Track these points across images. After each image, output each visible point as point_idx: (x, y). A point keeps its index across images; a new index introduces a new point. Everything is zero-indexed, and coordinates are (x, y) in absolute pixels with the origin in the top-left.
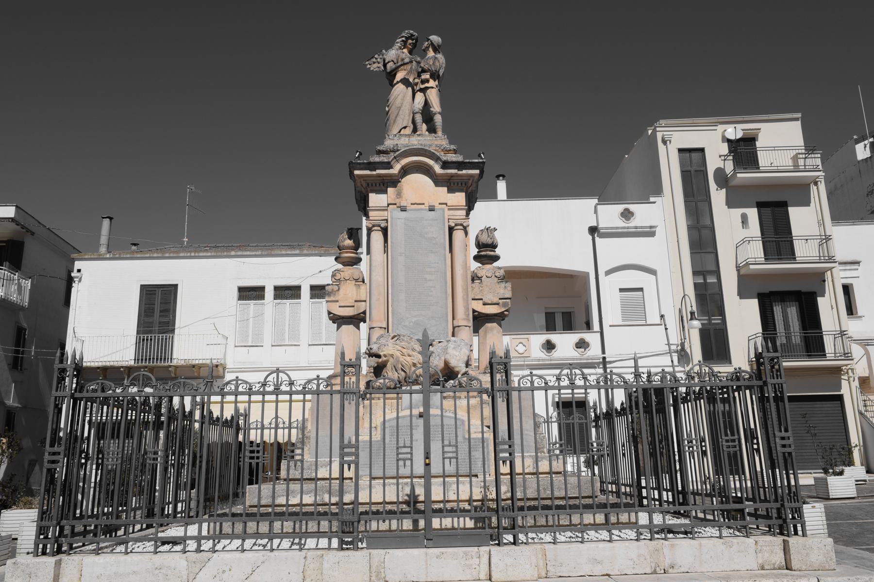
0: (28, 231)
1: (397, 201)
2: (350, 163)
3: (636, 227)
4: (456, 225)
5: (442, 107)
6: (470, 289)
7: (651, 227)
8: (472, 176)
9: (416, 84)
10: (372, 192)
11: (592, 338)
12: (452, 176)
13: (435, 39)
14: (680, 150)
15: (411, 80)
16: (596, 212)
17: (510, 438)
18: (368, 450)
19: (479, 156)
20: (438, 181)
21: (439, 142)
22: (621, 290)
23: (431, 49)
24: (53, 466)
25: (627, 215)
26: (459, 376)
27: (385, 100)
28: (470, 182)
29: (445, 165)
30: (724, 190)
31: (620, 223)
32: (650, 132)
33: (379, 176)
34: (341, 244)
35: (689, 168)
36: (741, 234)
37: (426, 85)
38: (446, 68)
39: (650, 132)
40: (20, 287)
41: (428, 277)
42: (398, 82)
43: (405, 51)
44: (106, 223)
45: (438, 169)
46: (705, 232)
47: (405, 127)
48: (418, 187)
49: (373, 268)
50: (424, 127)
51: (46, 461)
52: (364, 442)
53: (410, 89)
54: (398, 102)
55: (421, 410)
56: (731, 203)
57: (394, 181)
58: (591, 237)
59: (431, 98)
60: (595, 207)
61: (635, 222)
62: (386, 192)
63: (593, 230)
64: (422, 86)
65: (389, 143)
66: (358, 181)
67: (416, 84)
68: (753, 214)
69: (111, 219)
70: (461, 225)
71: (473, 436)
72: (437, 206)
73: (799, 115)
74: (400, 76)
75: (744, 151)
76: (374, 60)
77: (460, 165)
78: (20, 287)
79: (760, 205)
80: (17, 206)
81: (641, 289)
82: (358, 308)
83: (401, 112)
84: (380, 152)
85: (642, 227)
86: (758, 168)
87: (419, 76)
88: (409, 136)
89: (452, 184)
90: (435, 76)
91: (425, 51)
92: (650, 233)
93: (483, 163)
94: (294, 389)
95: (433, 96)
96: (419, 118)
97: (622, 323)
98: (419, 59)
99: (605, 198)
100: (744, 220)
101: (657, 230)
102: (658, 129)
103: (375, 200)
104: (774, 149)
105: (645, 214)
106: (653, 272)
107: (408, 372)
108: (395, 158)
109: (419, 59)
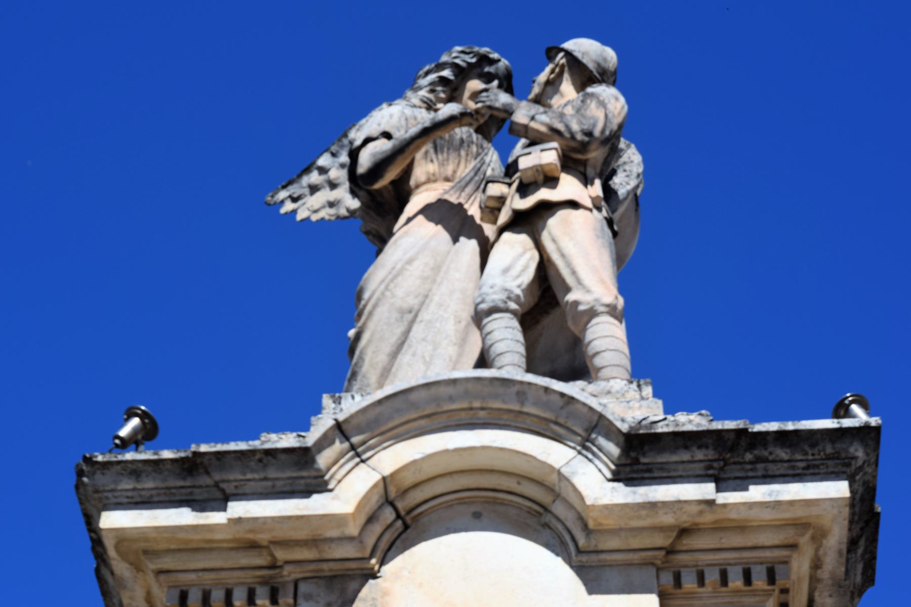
5: (624, 283)
28: (801, 566)
29: (640, 457)
33: (247, 539)
37: (544, 194)
45: (592, 482)
54: (405, 291)
59: (569, 247)
76: (314, 177)
77: (732, 457)
83: (417, 331)
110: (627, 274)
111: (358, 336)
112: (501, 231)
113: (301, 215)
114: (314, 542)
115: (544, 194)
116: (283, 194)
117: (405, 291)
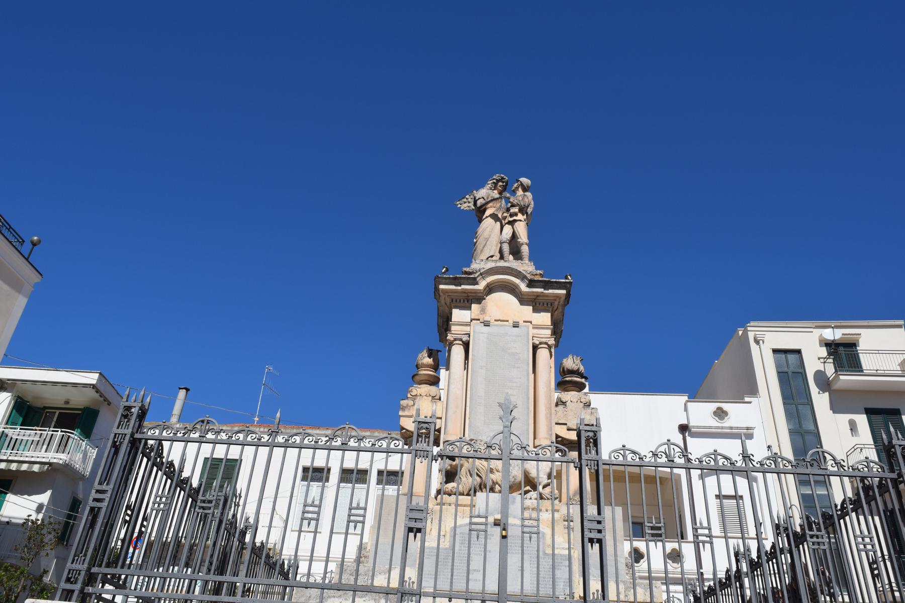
0: (105, 400)
1: (481, 317)
2: (436, 277)
3: (731, 428)
4: (541, 343)
6: (553, 412)
7: (748, 429)
8: (558, 296)
9: (505, 218)
10: (456, 307)
11: (688, 550)
12: (538, 295)
13: (525, 181)
14: (775, 351)
15: (500, 216)
16: (686, 410)
17: (599, 513)
18: (435, 558)
19: (566, 278)
20: (523, 300)
21: (526, 268)
23: (520, 189)
24: (98, 505)
25: (720, 414)
26: (540, 488)
27: (474, 234)
28: (556, 303)
30: (827, 394)
31: (713, 422)
32: (740, 333)
33: (464, 292)
34: (420, 362)
35: (786, 369)
36: (851, 442)
37: (515, 218)
38: (534, 208)
39: (740, 333)
40: (85, 454)
41: (510, 392)
43: (496, 192)
44: (182, 393)
45: (523, 287)
46: (808, 438)
47: (492, 256)
48: (501, 305)
49: (451, 381)
50: (511, 257)
51: (91, 498)
52: (430, 548)
53: (498, 223)
54: (486, 234)
55: (498, 517)
56: (836, 408)
57: (478, 298)
61: (728, 423)
62: (469, 308)
63: (684, 429)
64: (511, 219)
65: (475, 266)
66: (442, 298)
67: (505, 218)
68: (862, 420)
69: (187, 390)
70: (546, 343)
71: (556, 552)
72: (521, 323)
73: (902, 322)
74: (488, 213)
75: (844, 354)
77: (547, 285)
78: (85, 454)
79: (869, 412)
80: (100, 374)
84: (466, 273)
85: (737, 428)
86: (862, 371)
87: (508, 210)
88: (496, 261)
89: (538, 304)
90: (523, 210)
91: (514, 192)
93: (570, 283)
94: (362, 445)
95: (521, 229)
96: (506, 248)
98: (508, 195)
99: (694, 396)
100: (853, 427)
101: (755, 432)
102: (749, 329)
103: (458, 315)
104: (878, 352)
105: (739, 414)
107: (484, 477)
108: (481, 274)
109: (508, 195)
110: (530, 235)
115: (515, 218)
117: (486, 234)
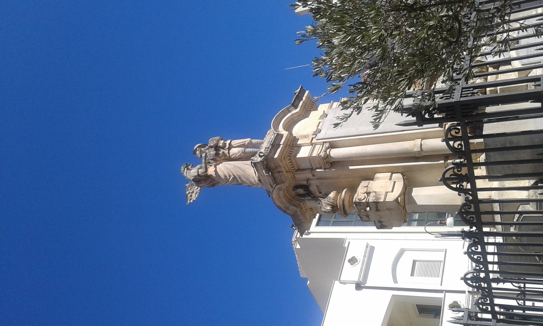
3: (365, 256)
7: (367, 247)
11: (450, 299)
22: (412, 274)
25: (353, 261)
32: (298, 246)
39: (298, 246)
42: (216, 171)
58: (364, 290)
60: (341, 283)
61: (360, 257)
63: (359, 286)
81: (414, 262)
82: (398, 179)
85: (365, 252)
92: (370, 250)
97: (440, 278)
106: (402, 252)
111: (234, 175)
112: (229, 153)
113: (195, 199)
114: (289, 140)
116: (188, 202)
